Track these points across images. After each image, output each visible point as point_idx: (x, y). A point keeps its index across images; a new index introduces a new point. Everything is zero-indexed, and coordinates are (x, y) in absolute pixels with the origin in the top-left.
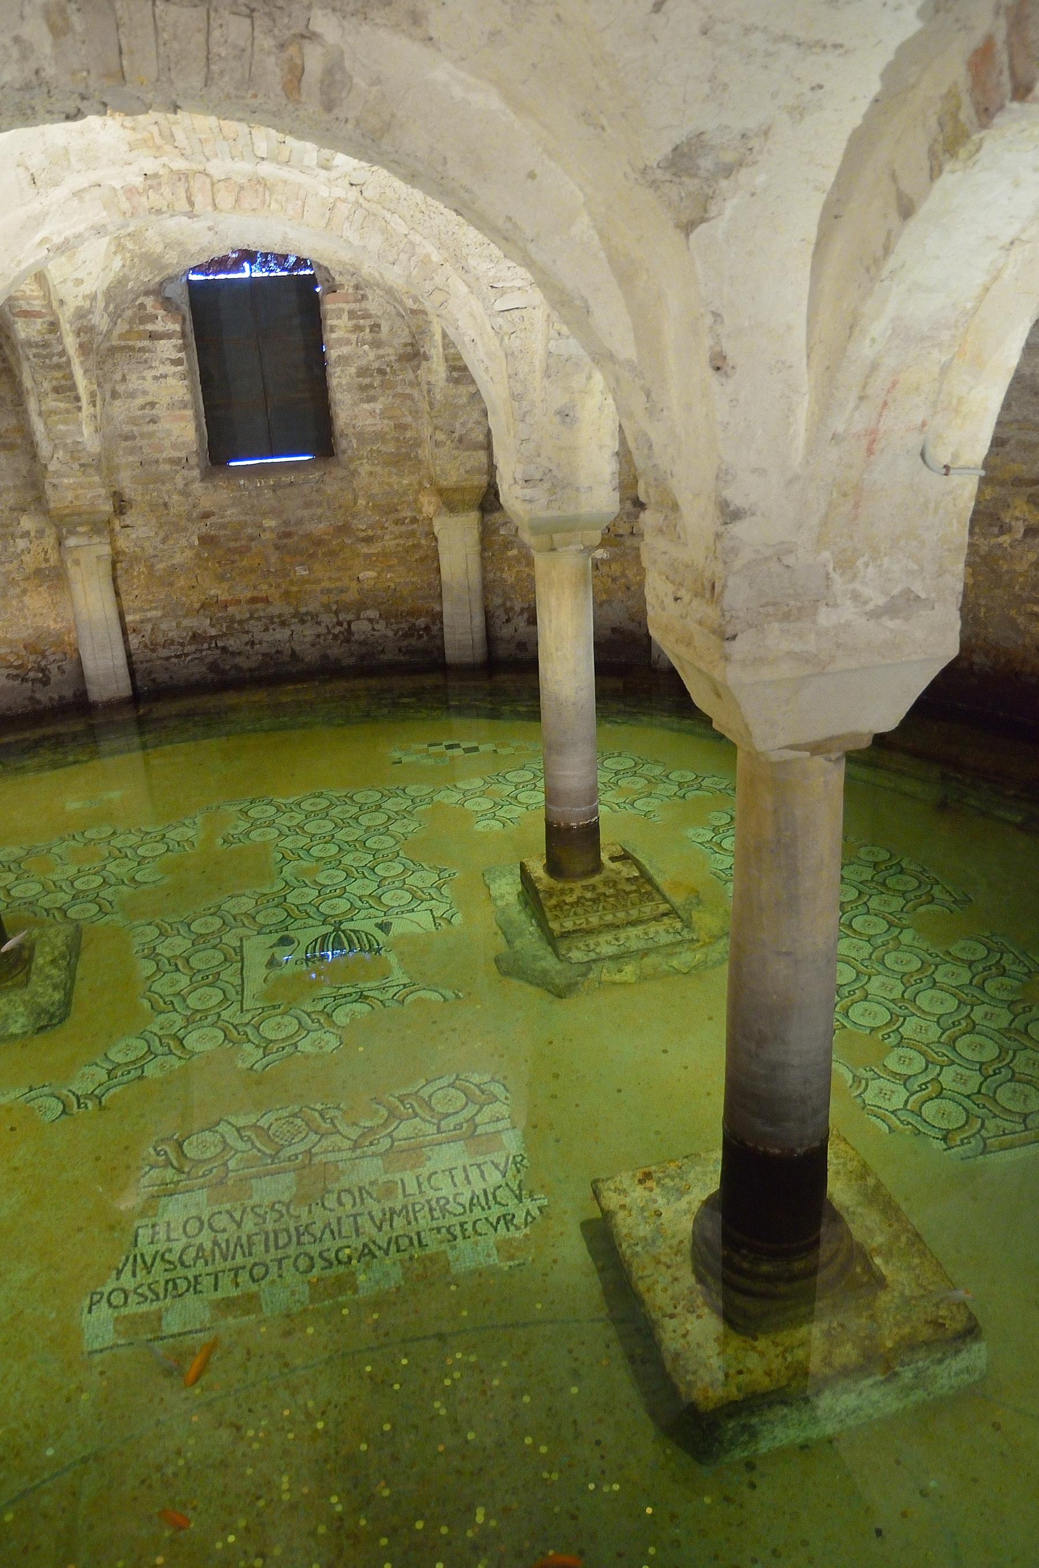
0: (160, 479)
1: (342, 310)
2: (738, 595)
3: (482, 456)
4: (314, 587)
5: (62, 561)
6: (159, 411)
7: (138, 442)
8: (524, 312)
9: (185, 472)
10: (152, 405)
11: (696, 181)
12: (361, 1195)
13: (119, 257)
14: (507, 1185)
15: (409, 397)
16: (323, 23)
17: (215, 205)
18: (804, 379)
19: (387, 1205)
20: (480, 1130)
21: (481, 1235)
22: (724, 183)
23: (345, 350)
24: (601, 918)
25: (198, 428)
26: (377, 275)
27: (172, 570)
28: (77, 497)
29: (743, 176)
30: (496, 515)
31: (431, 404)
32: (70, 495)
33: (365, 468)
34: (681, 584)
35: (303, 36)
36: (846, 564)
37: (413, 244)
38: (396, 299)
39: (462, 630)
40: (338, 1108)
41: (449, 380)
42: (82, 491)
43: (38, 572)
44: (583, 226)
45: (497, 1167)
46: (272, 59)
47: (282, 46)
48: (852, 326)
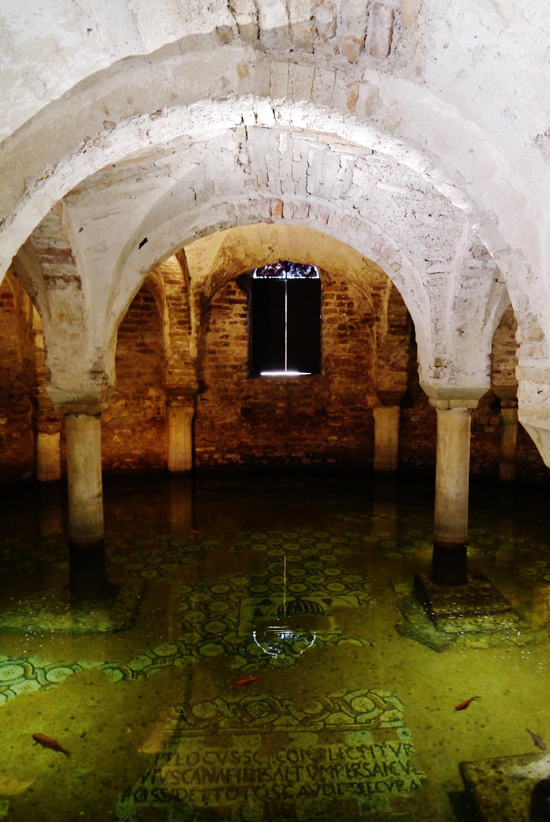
1: (333, 295)
4: (301, 442)
5: (168, 414)
6: (230, 340)
7: (217, 355)
9: (239, 373)
10: (227, 336)
13: (222, 258)
15: (366, 342)
21: (380, 792)
23: (332, 315)
25: (249, 352)
26: (355, 275)
27: (223, 426)
28: (181, 380)
30: (410, 409)
31: (378, 345)
32: (177, 378)
37: (383, 239)
38: (364, 290)
41: (389, 332)
42: (184, 377)
43: (153, 419)
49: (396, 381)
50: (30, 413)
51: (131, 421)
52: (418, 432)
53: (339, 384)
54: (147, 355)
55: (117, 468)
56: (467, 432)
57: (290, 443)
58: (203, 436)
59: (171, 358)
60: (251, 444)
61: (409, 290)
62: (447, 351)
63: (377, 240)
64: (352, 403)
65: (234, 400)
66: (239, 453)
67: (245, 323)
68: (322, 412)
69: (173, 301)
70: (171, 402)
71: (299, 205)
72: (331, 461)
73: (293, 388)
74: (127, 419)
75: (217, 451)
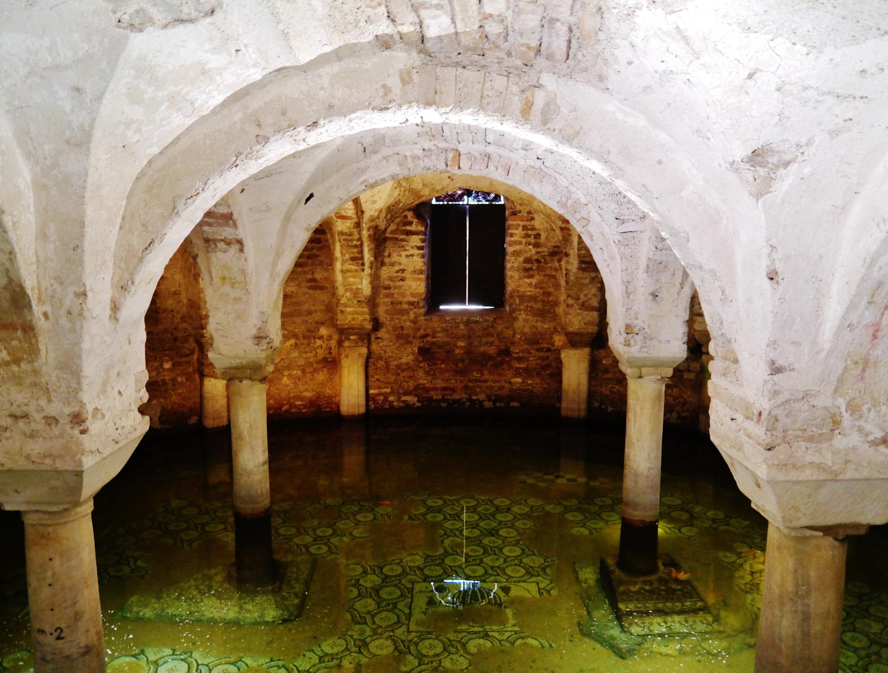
0: (403, 312)
1: (519, 225)
3: (595, 314)
5: (340, 354)
7: (392, 291)
9: (416, 310)
10: (403, 271)
11: (766, 170)
13: (398, 190)
15: (554, 277)
16: (547, 80)
23: (518, 247)
25: (427, 287)
27: (399, 367)
28: (353, 319)
29: (793, 167)
31: (567, 282)
32: (350, 317)
35: (535, 87)
41: (579, 268)
42: (356, 316)
43: (325, 360)
46: (517, 98)
50: (195, 356)
51: (301, 362)
52: (610, 376)
53: (524, 322)
54: (318, 292)
55: (286, 411)
56: (660, 401)
57: (471, 384)
58: (377, 377)
60: (428, 385)
61: (598, 247)
62: (639, 317)
65: (410, 339)
66: (416, 395)
67: (423, 256)
68: (505, 352)
71: (477, 155)
72: (515, 404)
73: (473, 326)
74: (297, 360)
75: (392, 392)
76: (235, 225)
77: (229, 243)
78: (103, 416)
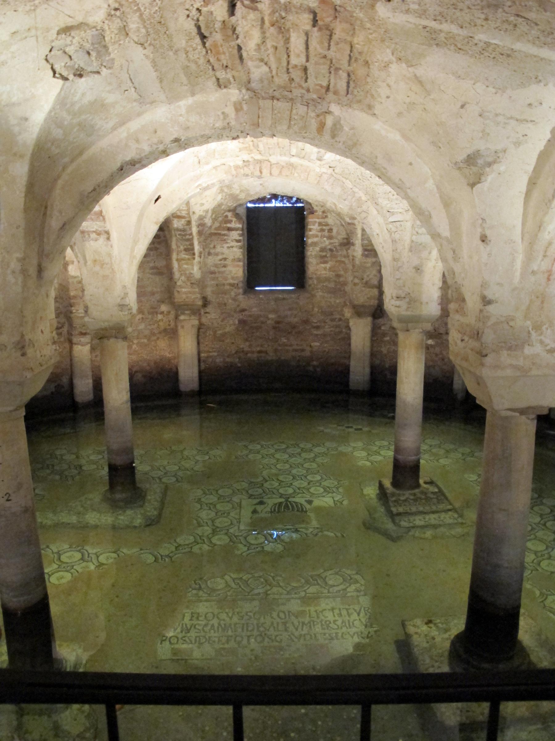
0: (225, 293)
1: (316, 222)
2: (489, 337)
3: (376, 292)
5: (176, 326)
6: (228, 262)
7: (217, 275)
8: (402, 223)
9: (235, 290)
10: (225, 259)
11: (477, 168)
12: (289, 615)
14: (360, 619)
15: (343, 262)
16: (334, 108)
17: (271, 174)
18: (520, 247)
19: (301, 620)
20: (349, 594)
21: (345, 639)
22: (487, 169)
23: (315, 240)
24: (417, 508)
25: (244, 272)
26: (334, 207)
27: (224, 335)
28: (187, 297)
29: (495, 166)
30: (380, 320)
31: (354, 266)
32: (184, 296)
33: (319, 294)
34: (465, 334)
35: (326, 113)
36: (537, 327)
37: (354, 192)
38: (341, 218)
39: (359, 373)
40: (281, 576)
41: (363, 255)
42: (190, 295)
43: (165, 330)
44: (430, 184)
45: (355, 611)
46: (314, 120)
47: (318, 116)
48: (540, 227)
49: (369, 296)
57: (280, 348)
59: (179, 279)
63: (349, 193)
64: (332, 314)
67: (241, 248)
69: (179, 233)
70: (180, 316)
71: (284, 164)
76: (104, 219)
77: (99, 234)
78: (34, 346)
